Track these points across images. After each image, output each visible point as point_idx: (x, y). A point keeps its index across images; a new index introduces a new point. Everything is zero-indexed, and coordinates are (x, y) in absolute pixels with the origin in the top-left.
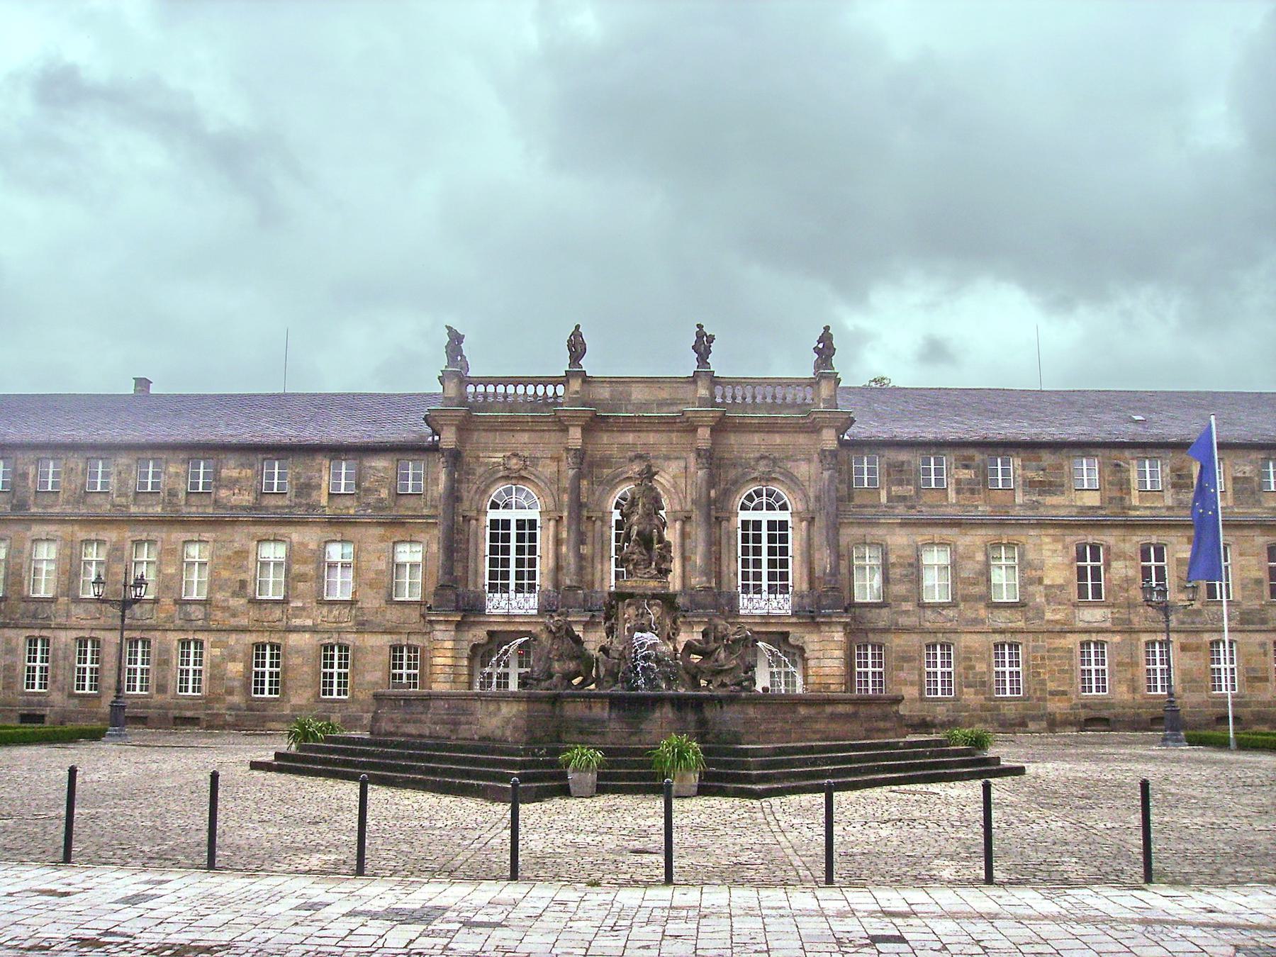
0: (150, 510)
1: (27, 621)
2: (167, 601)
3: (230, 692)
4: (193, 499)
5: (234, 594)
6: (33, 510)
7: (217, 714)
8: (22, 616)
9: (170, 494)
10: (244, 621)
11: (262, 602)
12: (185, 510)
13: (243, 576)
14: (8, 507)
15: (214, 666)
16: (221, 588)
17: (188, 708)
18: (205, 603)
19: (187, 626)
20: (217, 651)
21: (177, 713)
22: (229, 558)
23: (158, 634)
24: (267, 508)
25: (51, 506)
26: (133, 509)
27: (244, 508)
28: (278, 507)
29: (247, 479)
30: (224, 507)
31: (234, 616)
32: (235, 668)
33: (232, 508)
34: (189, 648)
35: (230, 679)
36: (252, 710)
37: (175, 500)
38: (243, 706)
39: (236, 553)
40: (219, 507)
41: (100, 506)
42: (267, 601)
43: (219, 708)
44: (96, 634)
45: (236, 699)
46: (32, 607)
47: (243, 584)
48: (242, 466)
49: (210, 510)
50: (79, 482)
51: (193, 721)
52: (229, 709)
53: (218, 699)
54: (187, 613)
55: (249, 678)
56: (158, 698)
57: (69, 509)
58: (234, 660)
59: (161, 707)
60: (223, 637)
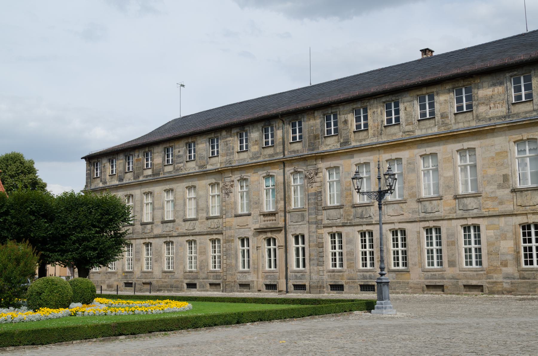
0: (430, 132)
1: (357, 221)
2: (449, 198)
3: (505, 264)
4: (460, 117)
5: (500, 186)
6: (354, 144)
7: (495, 282)
8: (355, 217)
9: (442, 117)
10: (509, 207)
11: (521, 191)
12: (454, 127)
13: (505, 172)
14: (339, 145)
15: (489, 244)
16: (489, 182)
17: (473, 278)
18: (476, 196)
19: (466, 215)
20: (491, 233)
21: (465, 282)
22: (493, 158)
23: (445, 222)
24: (517, 114)
25: (365, 140)
26: (418, 133)
27: (500, 118)
28: (526, 112)
29: (499, 94)
30: (484, 119)
31: (501, 203)
32: (507, 246)
33: (490, 119)
34: (469, 231)
35: (503, 254)
36: (524, 278)
37: (447, 121)
38: (517, 275)
39: (497, 154)
40: (480, 120)
41: (395, 134)
42: (527, 190)
43: (498, 277)
44: (402, 226)
45: (511, 270)
46: (359, 210)
47: (506, 178)
48: (494, 85)
49: (474, 124)
50: (379, 120)
51: (479, 288)
52: (505, 278)
53: (495, 270)
54: (465, 205)
55: (518, 253)
56: (449, 271)
57: (375, 140)
58: (505, 239)
59: (453, 278)
60: (495, 220)
